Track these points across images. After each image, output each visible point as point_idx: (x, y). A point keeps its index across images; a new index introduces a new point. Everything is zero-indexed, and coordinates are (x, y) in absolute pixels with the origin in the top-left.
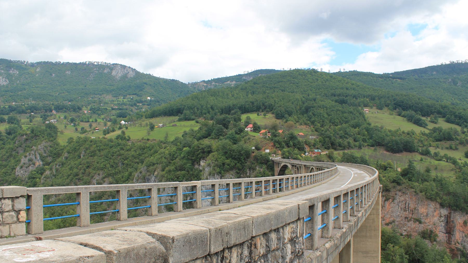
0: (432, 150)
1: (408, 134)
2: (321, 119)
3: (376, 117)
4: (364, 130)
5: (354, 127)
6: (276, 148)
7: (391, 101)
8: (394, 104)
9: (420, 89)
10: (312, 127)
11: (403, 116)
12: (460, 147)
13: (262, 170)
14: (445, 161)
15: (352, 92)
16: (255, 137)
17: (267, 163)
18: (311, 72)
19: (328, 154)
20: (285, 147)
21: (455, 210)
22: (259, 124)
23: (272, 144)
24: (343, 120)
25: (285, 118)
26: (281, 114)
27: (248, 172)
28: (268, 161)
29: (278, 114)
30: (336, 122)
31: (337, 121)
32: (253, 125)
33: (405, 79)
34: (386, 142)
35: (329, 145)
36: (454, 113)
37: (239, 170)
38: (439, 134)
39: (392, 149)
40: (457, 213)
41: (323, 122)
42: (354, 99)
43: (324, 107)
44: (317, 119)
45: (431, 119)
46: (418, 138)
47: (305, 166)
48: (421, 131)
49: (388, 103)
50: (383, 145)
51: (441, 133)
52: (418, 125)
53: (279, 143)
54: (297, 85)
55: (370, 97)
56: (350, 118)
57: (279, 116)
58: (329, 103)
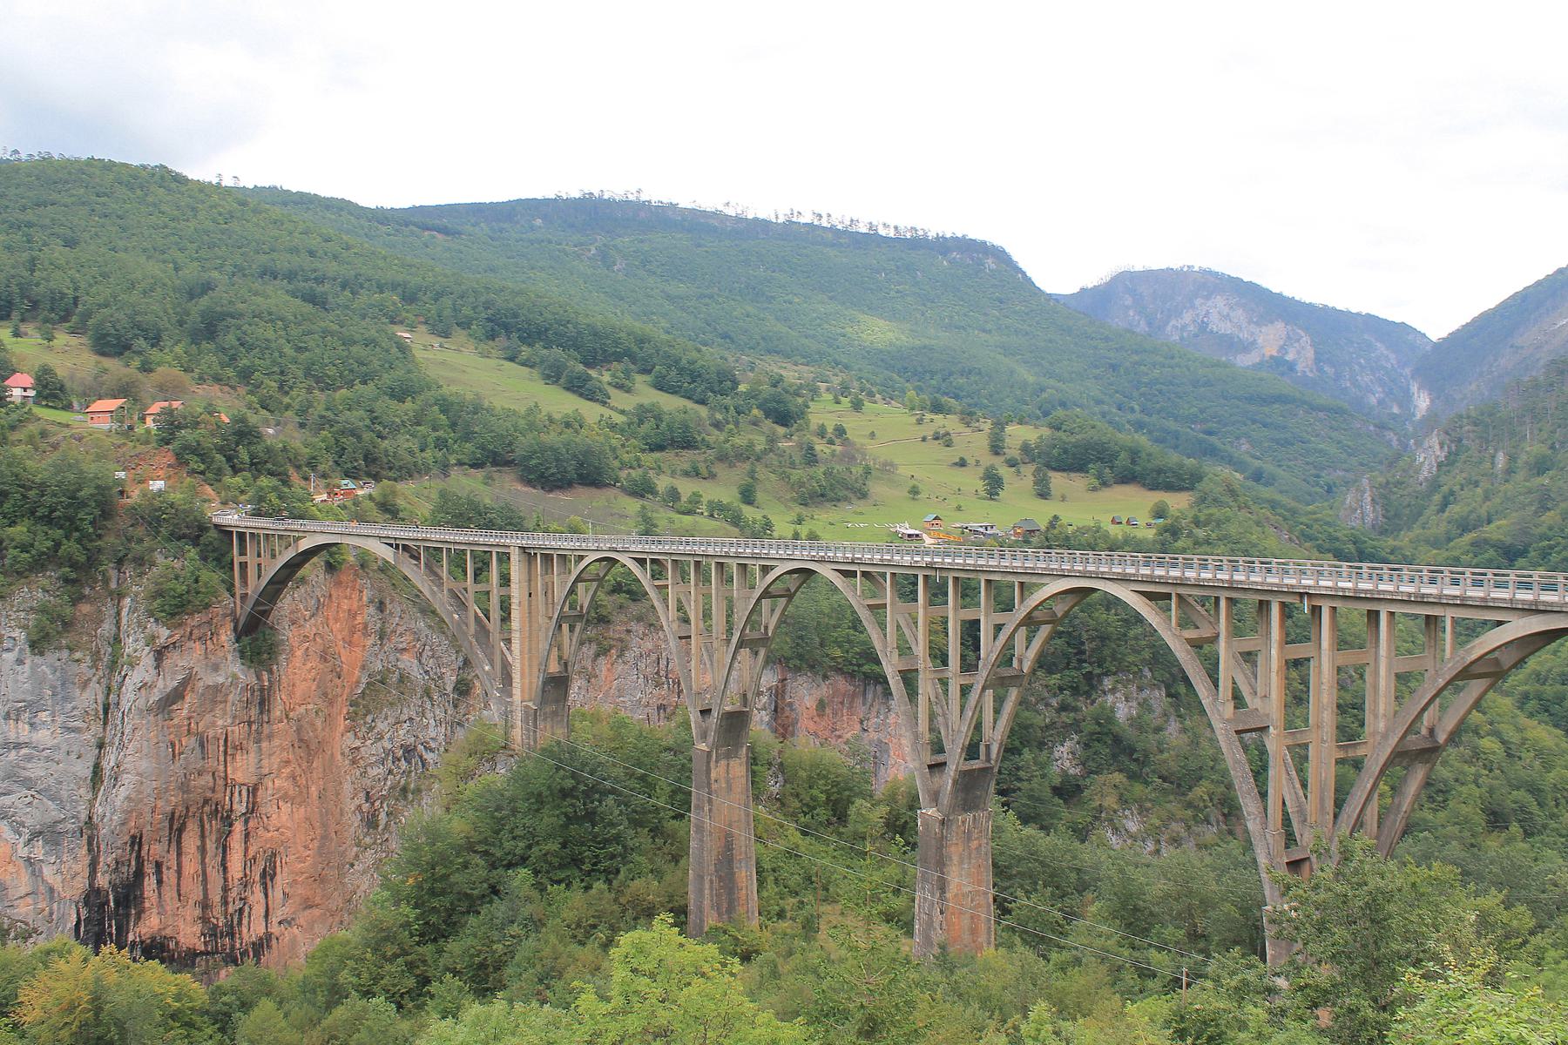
0: (662, 483)
1: (568, 425)
2: (274, 363)
3: (443, 363)
4: (436, 408)
5: (400, 393)
6: (193, 472)
7: (474, 308)
8: (489, 320)
9: (517, 272)
10: (242, 390)
11: (523, 364)
12: (719, 469)
13: (177, 564)
14: (706, 514)
15: (332, 268)
16: (68, 426)
17: (198, 537)
18: (162, 178)
19: (379, 499)
20: (228, 471)
21: (798, 669)
22: (61, 373)
23: (170, 459)
24: (351, 371)
25: (139, 353)
26: (118, 338)
27: (113, 574)
28: (202, 528)
29: (105, 336)
30: (329, 377)
31: (332, 371)
32: (38, 379)
33: (460, 233)
34: (519, 452)
35: (356, 461)
36: (677, 361)
37: (74, 566)
38: (658, 428)
39: (542, 475)
40: (800, 680)
41: (282, 373)
42: (347, 293)
43: (272, 318)
44: (257, 362)
45: (613, 376)
46: (597, 438)
47: (523, 548)
48: (602, 416)
49: (466, 317)
50: (508, 463)
51: (663, 425)
52: (581, 395)
53: (203, 456)
54: (119, 221)
55: (400, 290)
56: (376, 364)
57: (109, 345)
58: (277, 298)
